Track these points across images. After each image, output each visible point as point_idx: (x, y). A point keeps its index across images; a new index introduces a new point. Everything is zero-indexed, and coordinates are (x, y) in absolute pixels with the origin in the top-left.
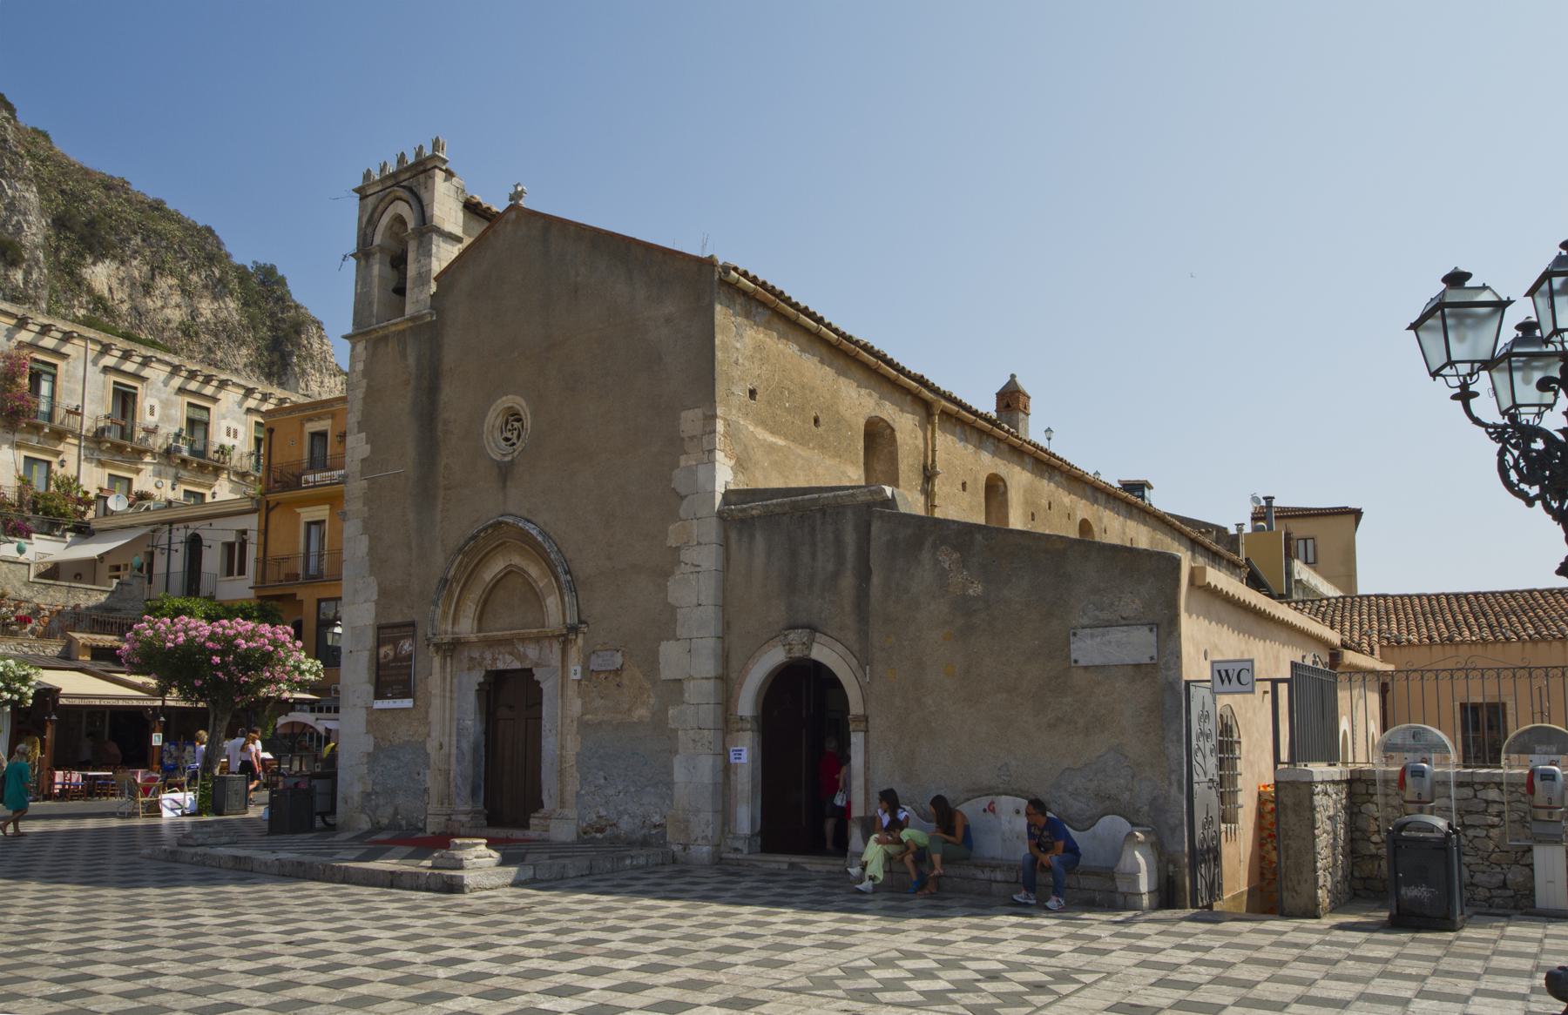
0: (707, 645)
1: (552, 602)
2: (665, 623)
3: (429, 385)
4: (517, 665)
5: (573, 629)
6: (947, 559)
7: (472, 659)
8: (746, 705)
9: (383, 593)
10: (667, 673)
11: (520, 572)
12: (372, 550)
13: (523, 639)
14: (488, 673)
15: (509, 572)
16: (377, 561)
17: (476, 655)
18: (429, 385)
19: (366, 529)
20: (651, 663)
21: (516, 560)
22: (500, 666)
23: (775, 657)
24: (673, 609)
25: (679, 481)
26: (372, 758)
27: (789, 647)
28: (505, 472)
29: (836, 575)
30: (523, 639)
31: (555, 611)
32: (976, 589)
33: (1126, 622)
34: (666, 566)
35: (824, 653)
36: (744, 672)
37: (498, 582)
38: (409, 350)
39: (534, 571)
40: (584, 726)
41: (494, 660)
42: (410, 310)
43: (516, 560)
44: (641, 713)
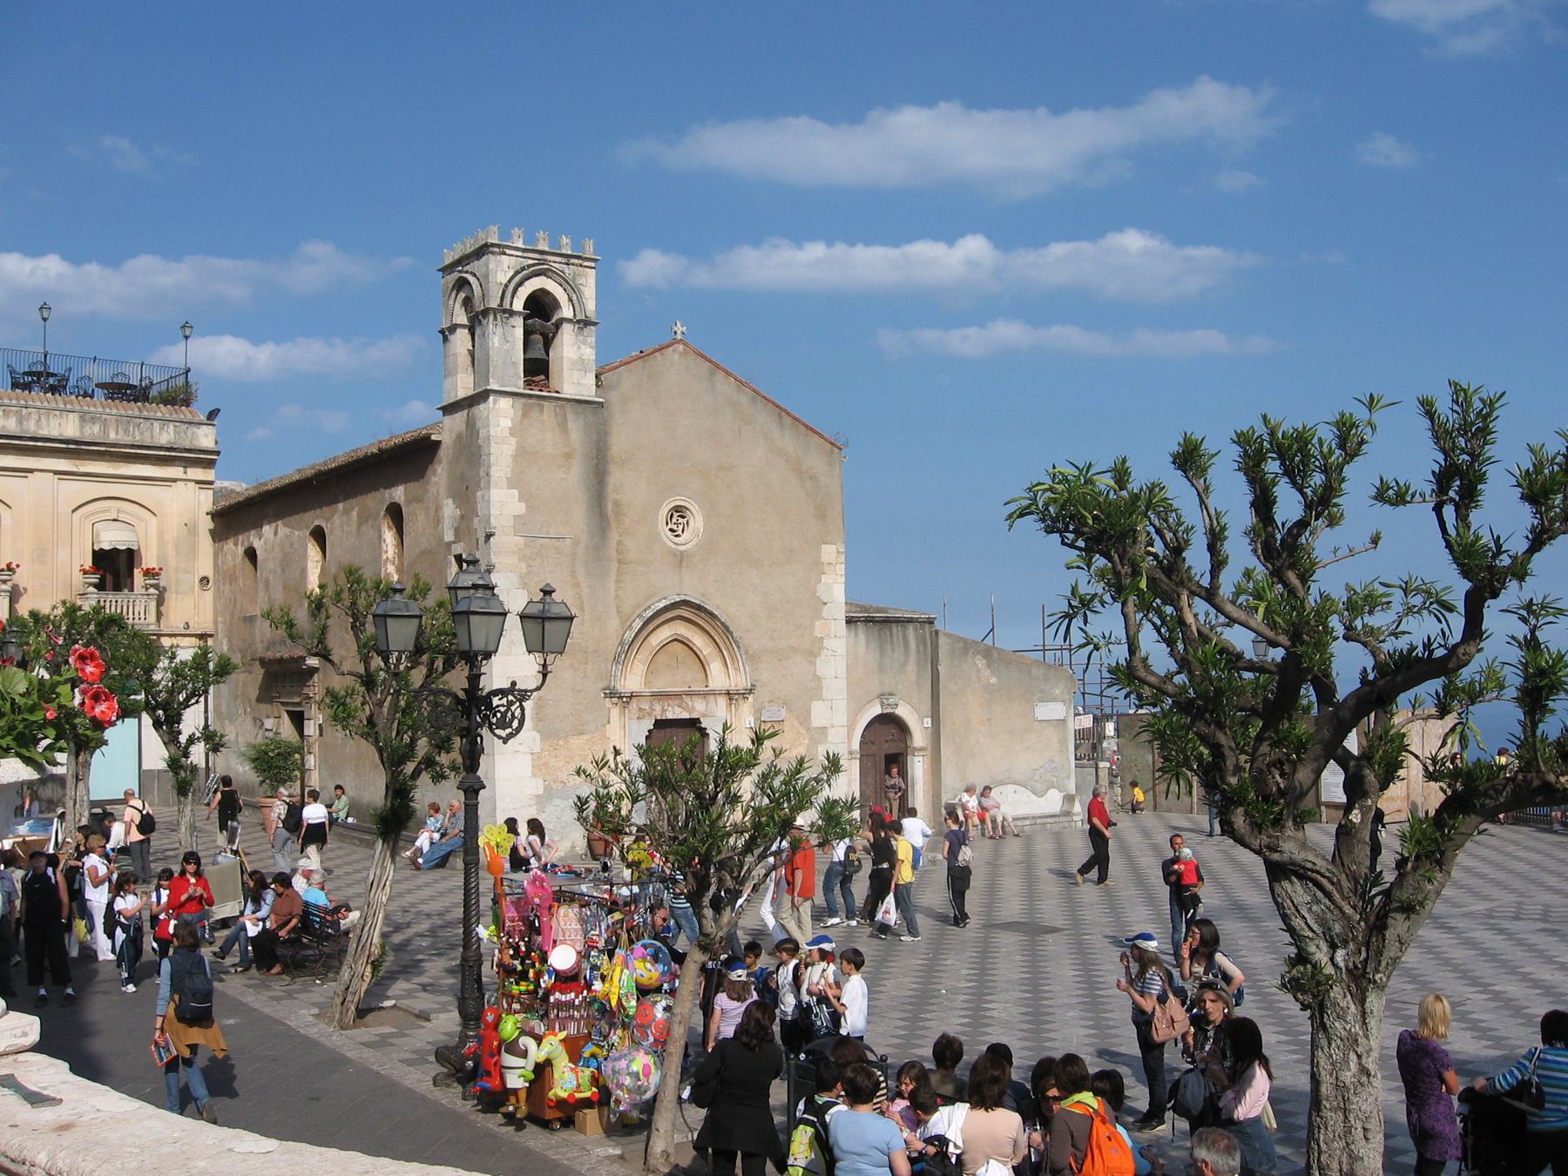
0: (842, 705)
1: (715, 667)
2: (815, 689)
4: (686, 715)
5: (751, 691)
6: (980, 662)
7: (641, 710)
10: (817, 721)
13: (691, 694)
14: (660, 724)
17: (646, 706)
20: (805, 718)
22: (670, 716)
23: (876, 710)
24: (818, 679)
25: (821, 592)
27: (882, 704)
28: (680, 559)
29: (904, 664)
30: (691, 694)
31: (719, 677)
32: (993, 680)
33: (1055, 700)
34: (813, 652)
35: (903, 711)
38: (571, 425)
39: (698, 640)
41: (664, 711)
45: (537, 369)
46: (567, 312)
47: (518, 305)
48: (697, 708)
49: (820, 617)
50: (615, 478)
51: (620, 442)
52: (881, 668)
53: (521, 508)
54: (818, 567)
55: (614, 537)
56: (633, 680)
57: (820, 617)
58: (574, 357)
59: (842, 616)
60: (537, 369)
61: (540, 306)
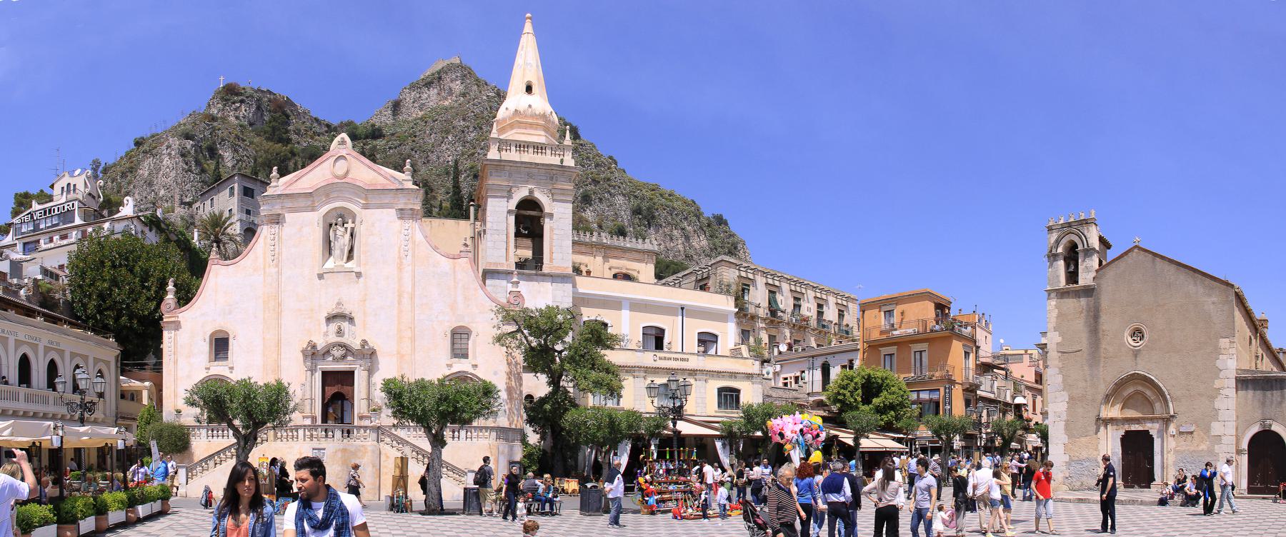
1: (1158, 406)
2: (1214, 415)
3: (1094, 316)
8: (1245, 445)
9: (1071, 398)
11: (1142, 394)
12: (1064, 380)
15: (1137, 392)
16: (1067, 385)
18: (1094, 316)
19: (1061, 372)
20: (1207, 429)
21: (1140, 388)
24: (1217, 410)
25: (1219, 364)
26: (1068, 464)
28: (1136, 354)
34: (1214, 394)
35: (1276, 428)
36: (1244, 433)
37: (1130, 397)
39: (1148, 393)
40: (1176, 452)
42: (1081, 282)
43: (1140, 388)
44: (1203, 447)
45: (1072, 276)
46: (1080, 247)
47: (1060, 250)
48: (1148, 426)
49: (1218, 377)
50: (1104, 318)
51: (1105, 301)
52: (1263, 404)
53: (1059, 339)
54: (1217, 351)
55: (1103, 345)
56: (1114, 412)
57: (1218, 377)
58: (1088, 270)
59: (1233, 375)
60: (1072, 276)
61: (1073, 247)
